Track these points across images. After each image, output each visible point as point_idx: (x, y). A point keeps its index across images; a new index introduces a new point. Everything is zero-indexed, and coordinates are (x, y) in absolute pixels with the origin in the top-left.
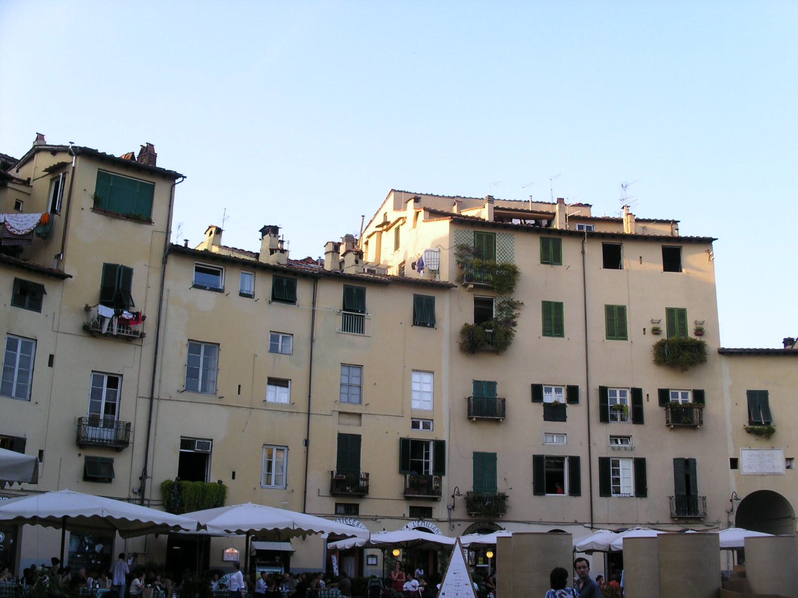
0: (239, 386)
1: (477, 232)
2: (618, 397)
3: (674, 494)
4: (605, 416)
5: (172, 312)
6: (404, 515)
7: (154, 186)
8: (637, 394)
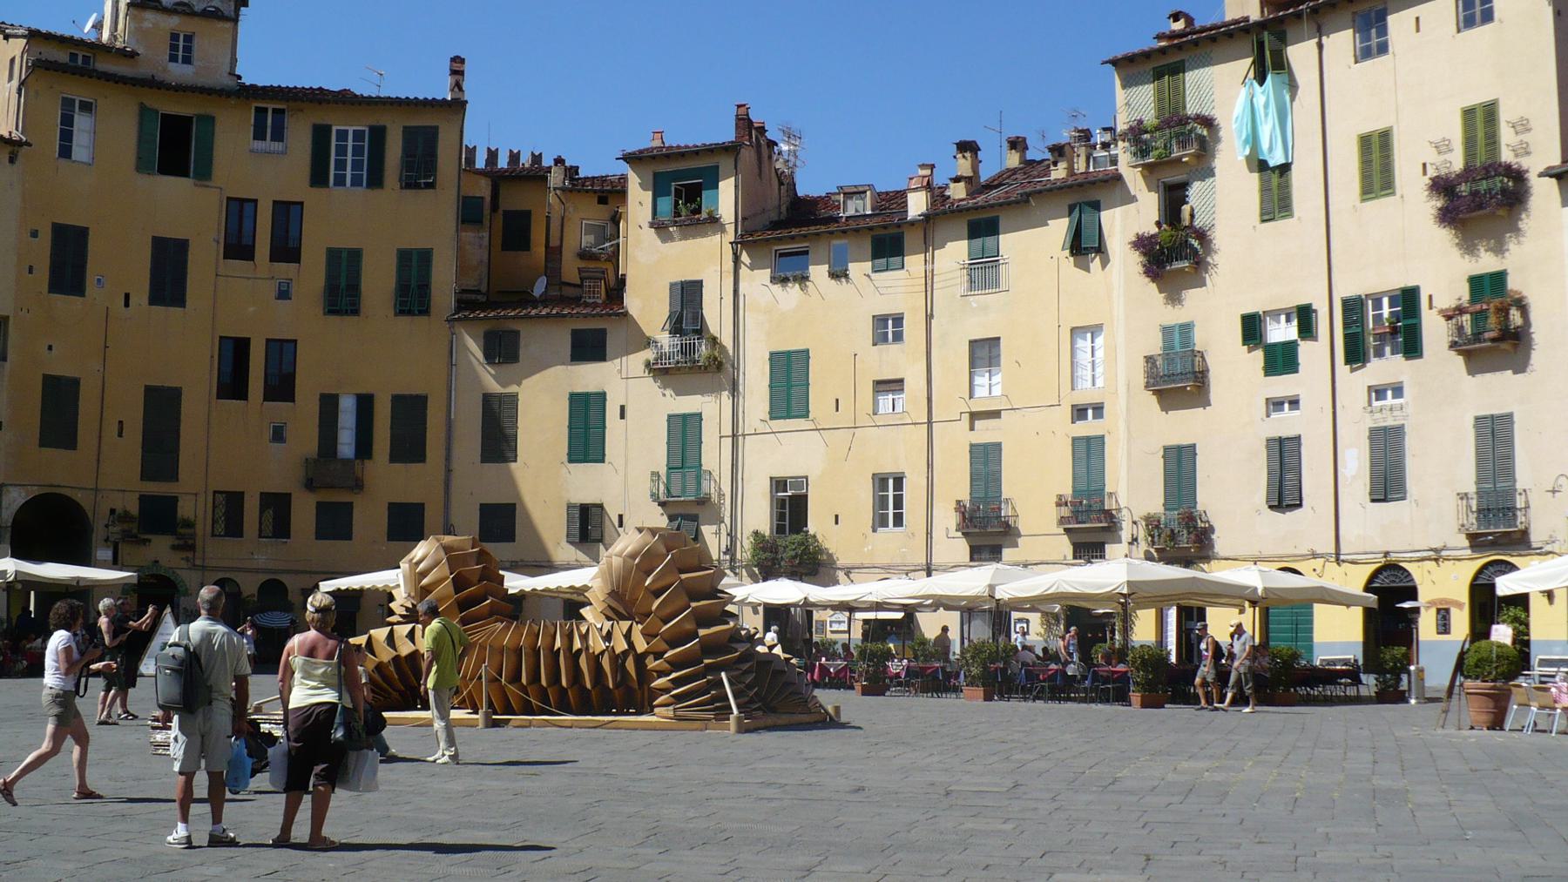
0: (837, 400)
1: (1156, 68)
4: (1356, 354)
5: (750, 320)
6: (1065, 556)
7: (718, 167)
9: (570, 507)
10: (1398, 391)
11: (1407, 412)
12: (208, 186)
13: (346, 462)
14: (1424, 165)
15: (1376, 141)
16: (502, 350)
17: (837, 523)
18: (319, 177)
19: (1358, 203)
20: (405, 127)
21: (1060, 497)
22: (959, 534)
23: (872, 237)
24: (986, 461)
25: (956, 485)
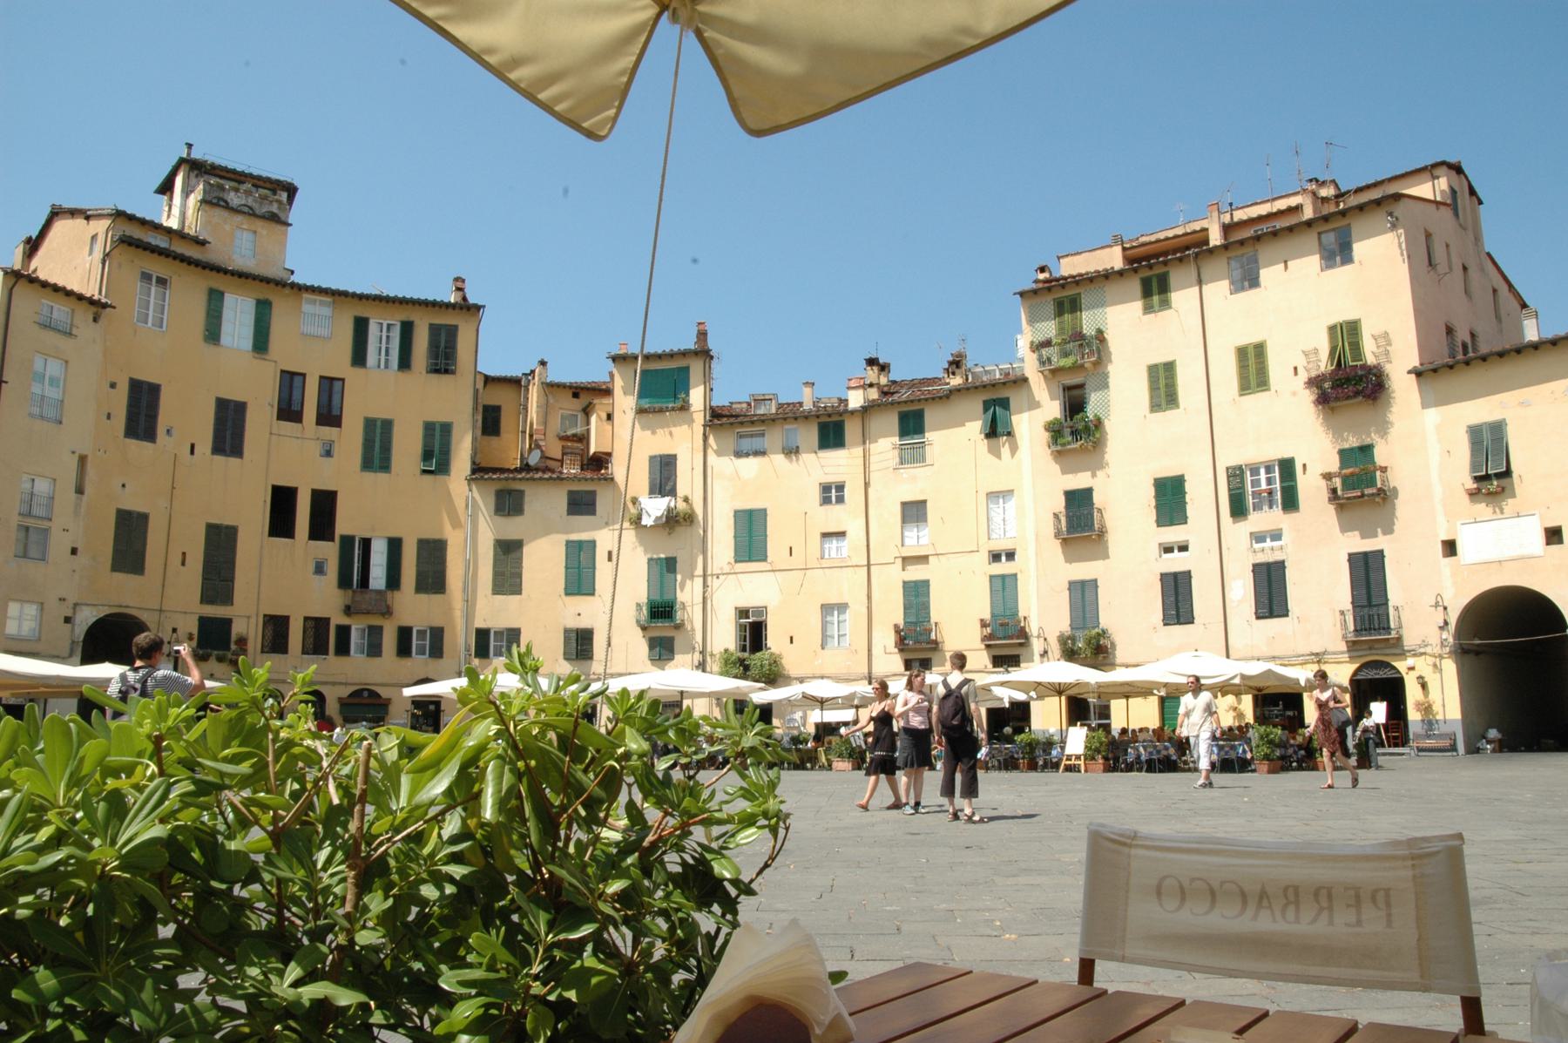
2: (1263, 476)
3: (1350, 607)
4: (1238, 509)
8: (1287, 468)
9: (567, 631)
10: (1277, 536)
11: (1289, 551)
12: (265, 359)
13: (378, 592)
14: (1296, 369)
15: (1251, 353)
17: (792, 642)
18: (359, 358)
19: (1237, 397)
20: (431, 325)
21: (982, 620)
22: (896, 650)
23: (819, 423)
24: (916, 594)
25: (892, 612)
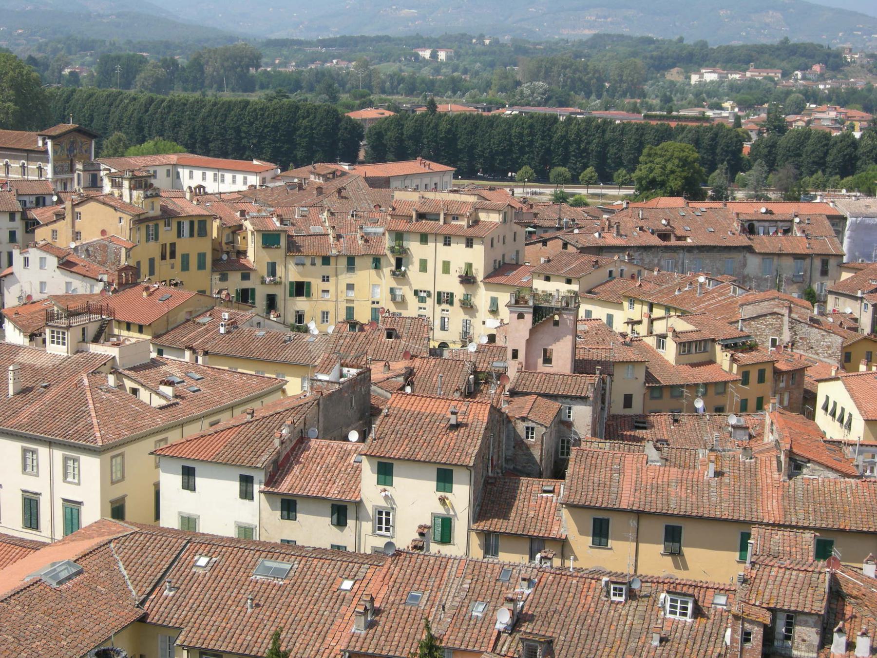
8: (452, 295)
16: (224, 278)
18: (179, 234)
24: (350, 311)
